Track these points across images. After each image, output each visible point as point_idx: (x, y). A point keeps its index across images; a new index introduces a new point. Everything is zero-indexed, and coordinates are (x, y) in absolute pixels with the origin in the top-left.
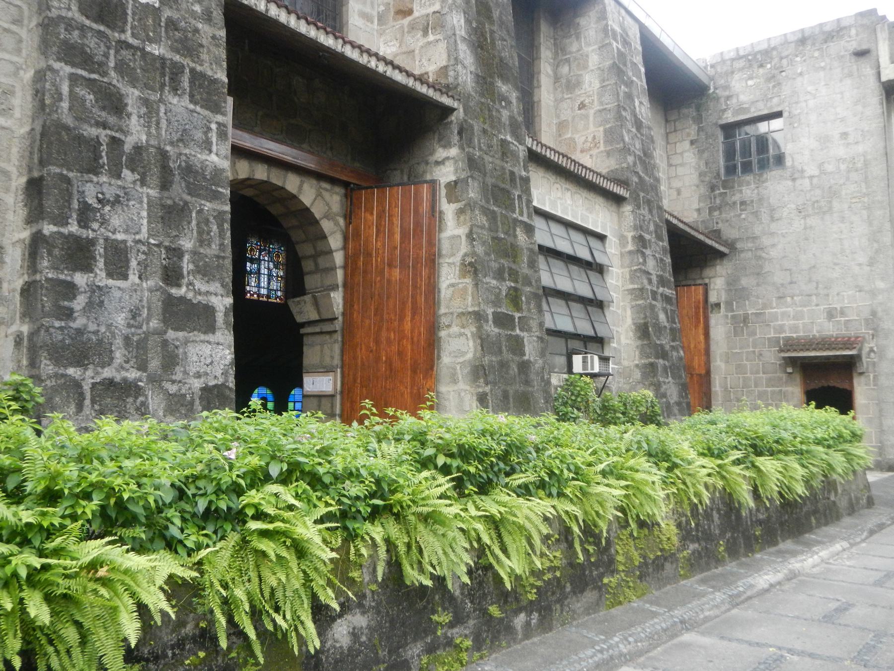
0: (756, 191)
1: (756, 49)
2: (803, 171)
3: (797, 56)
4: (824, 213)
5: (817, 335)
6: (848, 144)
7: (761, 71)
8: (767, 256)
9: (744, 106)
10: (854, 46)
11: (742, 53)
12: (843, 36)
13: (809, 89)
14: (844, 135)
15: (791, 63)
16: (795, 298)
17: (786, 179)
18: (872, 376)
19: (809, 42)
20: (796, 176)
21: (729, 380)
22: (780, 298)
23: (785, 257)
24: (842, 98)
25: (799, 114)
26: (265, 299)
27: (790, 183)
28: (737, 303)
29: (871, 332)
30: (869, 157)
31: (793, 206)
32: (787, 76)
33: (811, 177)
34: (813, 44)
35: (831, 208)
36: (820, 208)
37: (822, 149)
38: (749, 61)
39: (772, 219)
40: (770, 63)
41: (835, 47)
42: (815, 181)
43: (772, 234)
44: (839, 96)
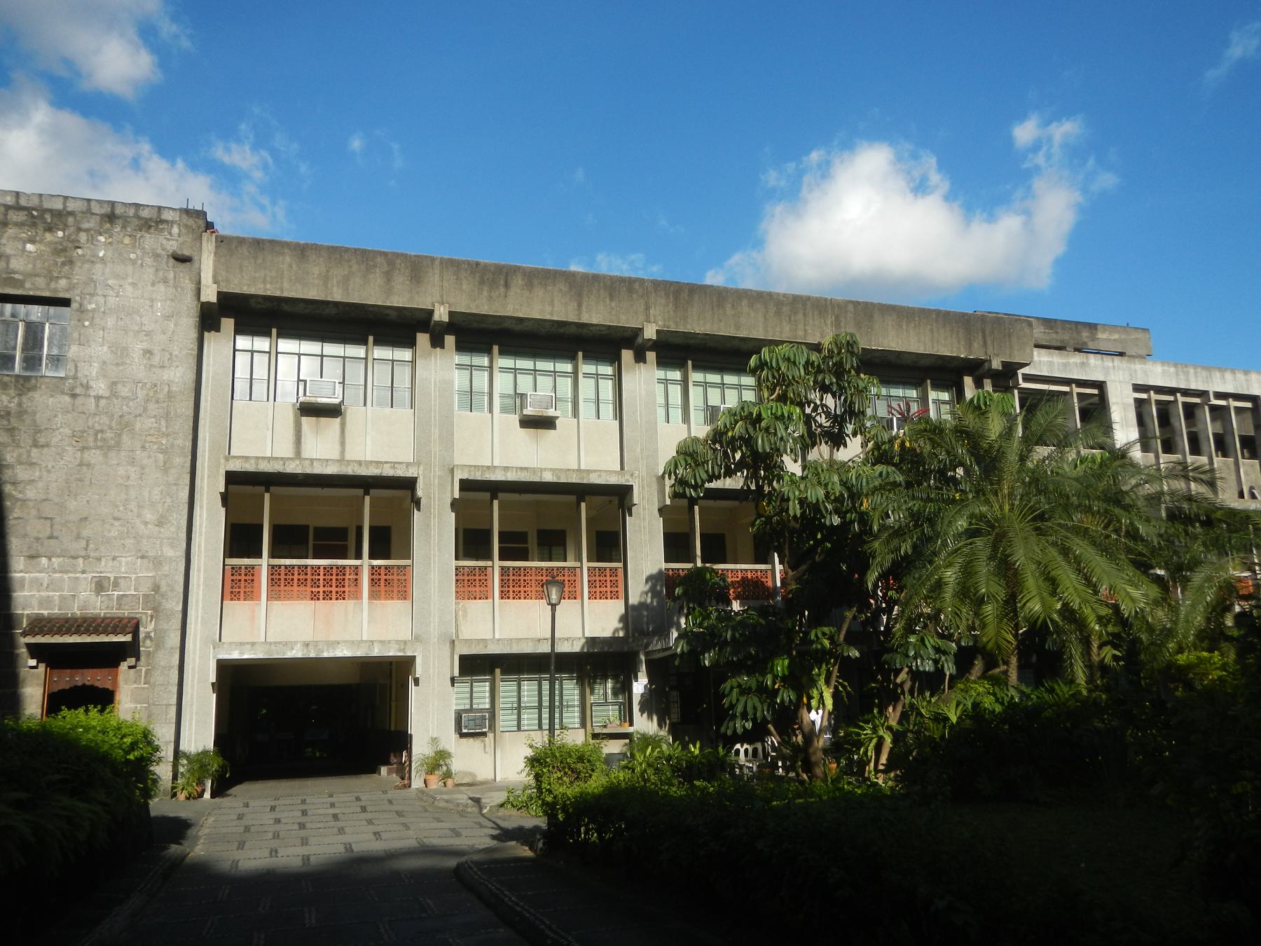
0: (16, 400)
1: (47, 205)
2: (87, 387)
3: (101, 234)
4: (110, 448)
5: (78, 613)
6: (151, 365)
7: (48, 236)
8: (20, 496)
9: (17, 276)
10: (172, 246)
11: (23, 202)
13: (110, 282)
14: (148, 353)
15: (92, 240)
16: (53, 560)
17: (63, 393)
18: (144, 669)
19: (120, 222)
20: (78, 391)
22: (32, 557)
23: (44, 500)
24: (151, 306)
25: (94, 310)
27: (67, 399)
29: (149, 612)
30: (174, 389)
31: (68, 431)
32: (83, 255)
33: (98, 398)
34: (124, 227)
35: (118, 445)
36: (103, 440)
37: (117, 364)
38: (33, 216)
39: (35, 444)
40: (64, 230)
41: (150, 240)
42: (103, 402)
43: (32, 464)
44: (148, 302)
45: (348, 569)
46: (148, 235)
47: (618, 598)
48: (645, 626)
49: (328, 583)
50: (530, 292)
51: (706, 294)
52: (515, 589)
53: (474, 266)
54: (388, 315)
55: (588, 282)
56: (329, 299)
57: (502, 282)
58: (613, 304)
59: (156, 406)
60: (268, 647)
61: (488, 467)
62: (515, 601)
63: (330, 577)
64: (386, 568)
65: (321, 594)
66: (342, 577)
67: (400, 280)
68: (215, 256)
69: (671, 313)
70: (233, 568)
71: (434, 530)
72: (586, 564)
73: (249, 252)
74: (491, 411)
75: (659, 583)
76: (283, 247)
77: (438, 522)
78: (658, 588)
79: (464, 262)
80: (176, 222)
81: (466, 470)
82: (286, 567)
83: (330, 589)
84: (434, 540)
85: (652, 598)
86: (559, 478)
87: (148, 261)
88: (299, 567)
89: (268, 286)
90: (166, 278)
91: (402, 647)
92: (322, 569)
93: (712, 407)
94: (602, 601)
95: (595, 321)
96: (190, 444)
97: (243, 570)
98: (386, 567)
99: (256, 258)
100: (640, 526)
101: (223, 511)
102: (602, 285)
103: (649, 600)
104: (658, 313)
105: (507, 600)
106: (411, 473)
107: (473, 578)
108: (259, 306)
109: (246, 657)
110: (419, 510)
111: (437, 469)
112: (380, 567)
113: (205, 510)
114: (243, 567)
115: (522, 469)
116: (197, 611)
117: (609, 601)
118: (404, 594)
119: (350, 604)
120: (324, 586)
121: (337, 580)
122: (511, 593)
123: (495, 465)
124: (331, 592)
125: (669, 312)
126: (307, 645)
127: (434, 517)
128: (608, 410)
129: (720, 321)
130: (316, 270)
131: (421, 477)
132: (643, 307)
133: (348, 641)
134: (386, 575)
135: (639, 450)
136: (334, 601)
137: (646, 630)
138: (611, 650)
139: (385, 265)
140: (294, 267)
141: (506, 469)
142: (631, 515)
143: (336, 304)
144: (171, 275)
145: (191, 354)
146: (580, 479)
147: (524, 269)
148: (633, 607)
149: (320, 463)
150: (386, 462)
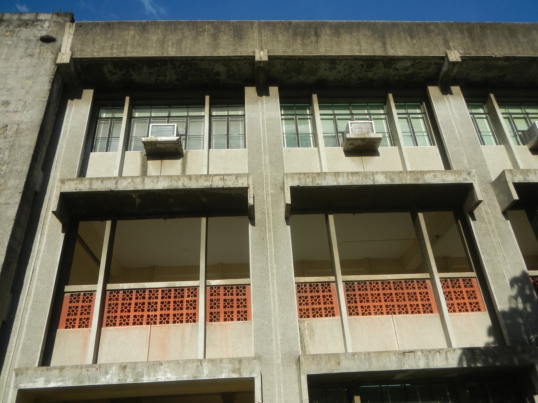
6: (7, 111)
12: (36, 26)
19: (5, 24)
24: (17, 72)
30: (23, 126)
34: (8, 26)
41: (25, 32)
45: (186, 291)
46: (24, 29)
47: (479, 310)
48: (525, 337)
49: (165, 306)
50: (338, 38)
51: (496, 29)
52: (363, 304)
53: (288, 25)
54: (218, 74)
55: (388, 27)
56: (165, 55)
57: (312, 33)
58: (414, 41)
59: (4, 140)
60: (78, 371)
61: (318, 174)
62: (365, 317)
63: (168, 300)
64: (225, 288)
65: (158, 317)
66: (180, 299)
67: (225, 39)
68: (74, 35)
69: (470, 44)
70: (72, 295)
71: (270, 243)
72: (437, 276)
73: (101, 31)
74: (316, 144)
75: (527, 287)
76: (129, 25)
77: (274, 235)
78: (528, 292)
79: (278, 23)
80: (48, 20)
81: (296, 177)
82: (124, 291)
83: (167, 312)
84: (271, 252)
85: (524, 302)
86: (392, 180)
87: (22, 44)
88: (138, 290)
89: (115, 51)
90: (33, 53)
91: (237, 367)
92: (160, 292)
93: (523, 132)
94: (462, 313)
95: (400, 54)
96: (28, 168)
97: (81, 297)
98: (225, 287)
99: (106, 34)
100: (487, 229)
101: (62, 236)
102: (401, 29)
103: (521, 306)
104: (457, 44)
105: (356, 317)
106: (241, 183)
107: (316, 294)
108: (115, 78)
109: (52, 385)
110: (253, 224)
111: (269, 188)
112: (218, 287)
113: (45, 236)
114: (82, 293)
115: (352, 173)
116: (19, 338)
117: (470, 314)
118: (244, 316)
119: (188, 327)
120: (161, 309)
121: (175, 302)
122: (359, 309)
123: (324, 171)
124: (168, 315)
125: (467, 43)
126: (124, 367)
127: (270, 231)
128: (424, 139)
129: (517, 46)
130: (155, 38)
131: (251, 187)
132: (441, 42)
133: (172, 361)
134: (225, 295)
135: (466, 161)
136: (171, 324)
137: (527, 342)
138: (498, 364)
139: (212, 30)
140: (137, 37)
141: (337, 174)
142: (474, 219)
143: (172, 60)
144: (38, 50)
145: (42, 101)
146: (415, 180)
147: (330, 23)
148: (504, 313)
149: (151, 179)
150: (216, 175)
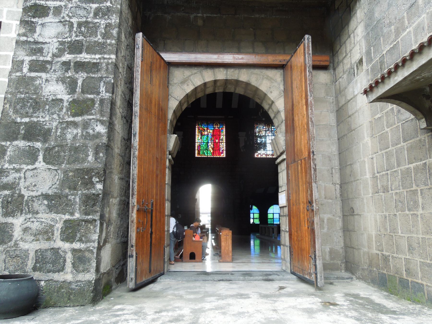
21: (375, 159)
26: (270, 157)
28: (374, 46)
